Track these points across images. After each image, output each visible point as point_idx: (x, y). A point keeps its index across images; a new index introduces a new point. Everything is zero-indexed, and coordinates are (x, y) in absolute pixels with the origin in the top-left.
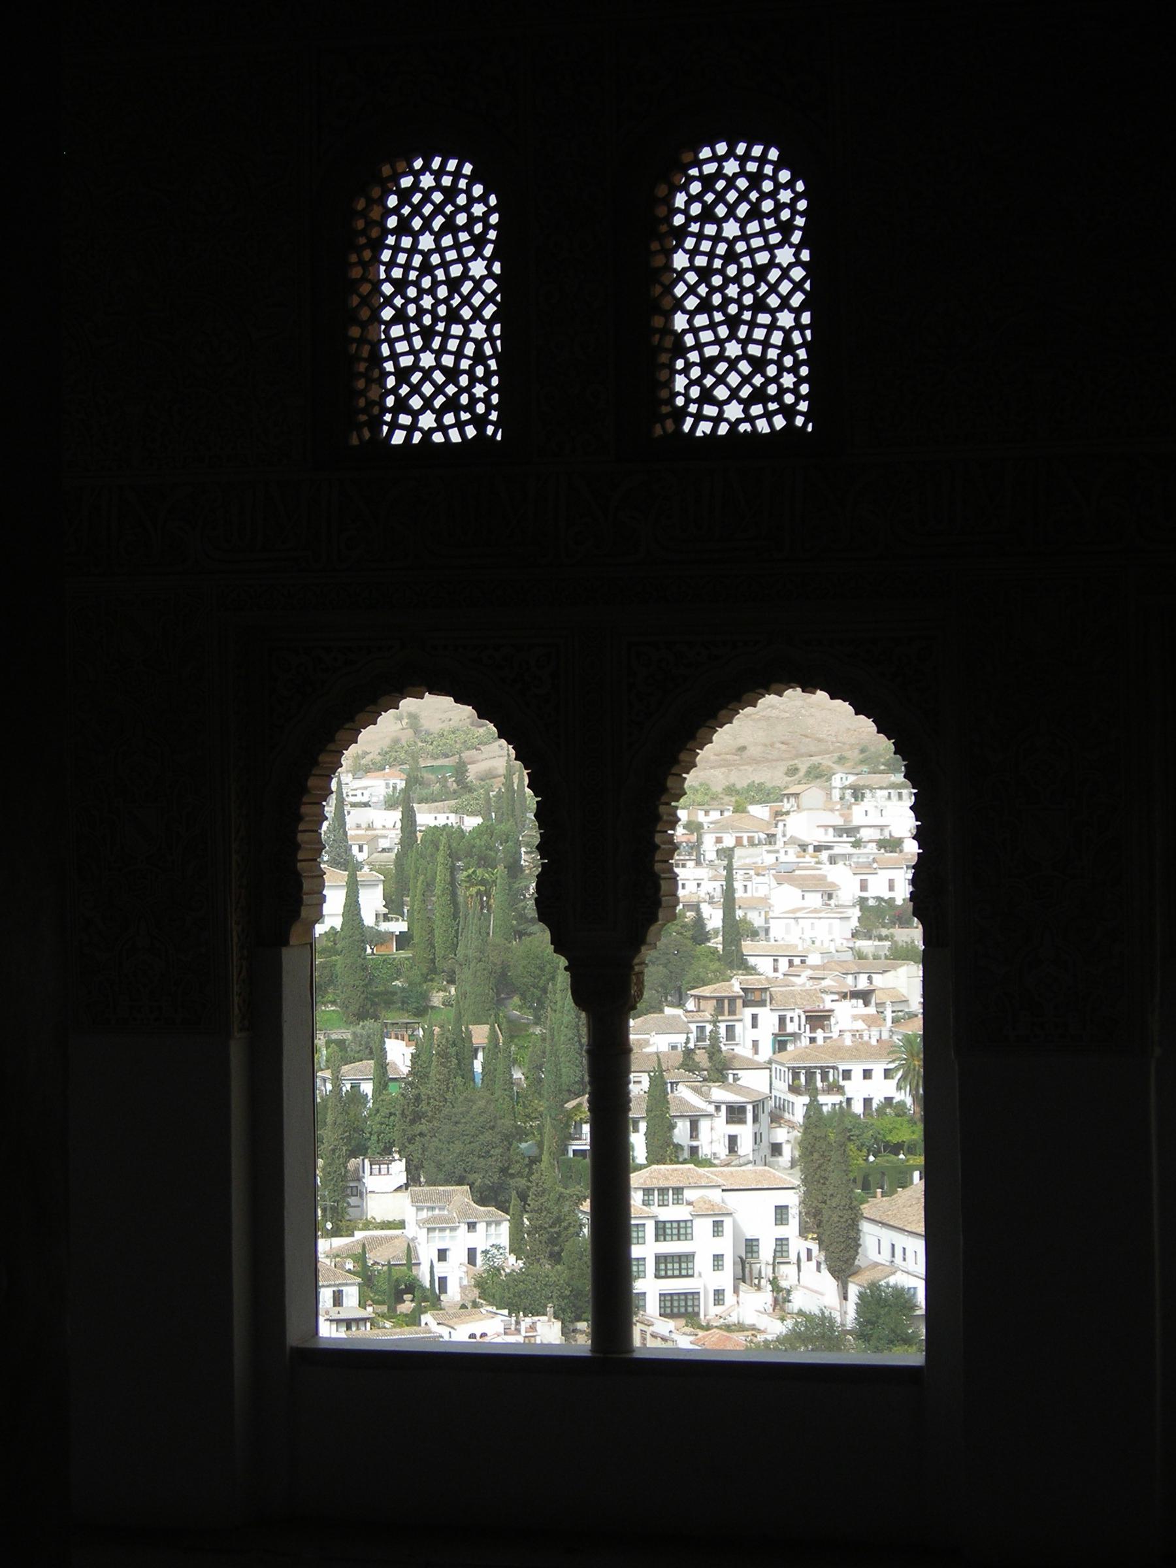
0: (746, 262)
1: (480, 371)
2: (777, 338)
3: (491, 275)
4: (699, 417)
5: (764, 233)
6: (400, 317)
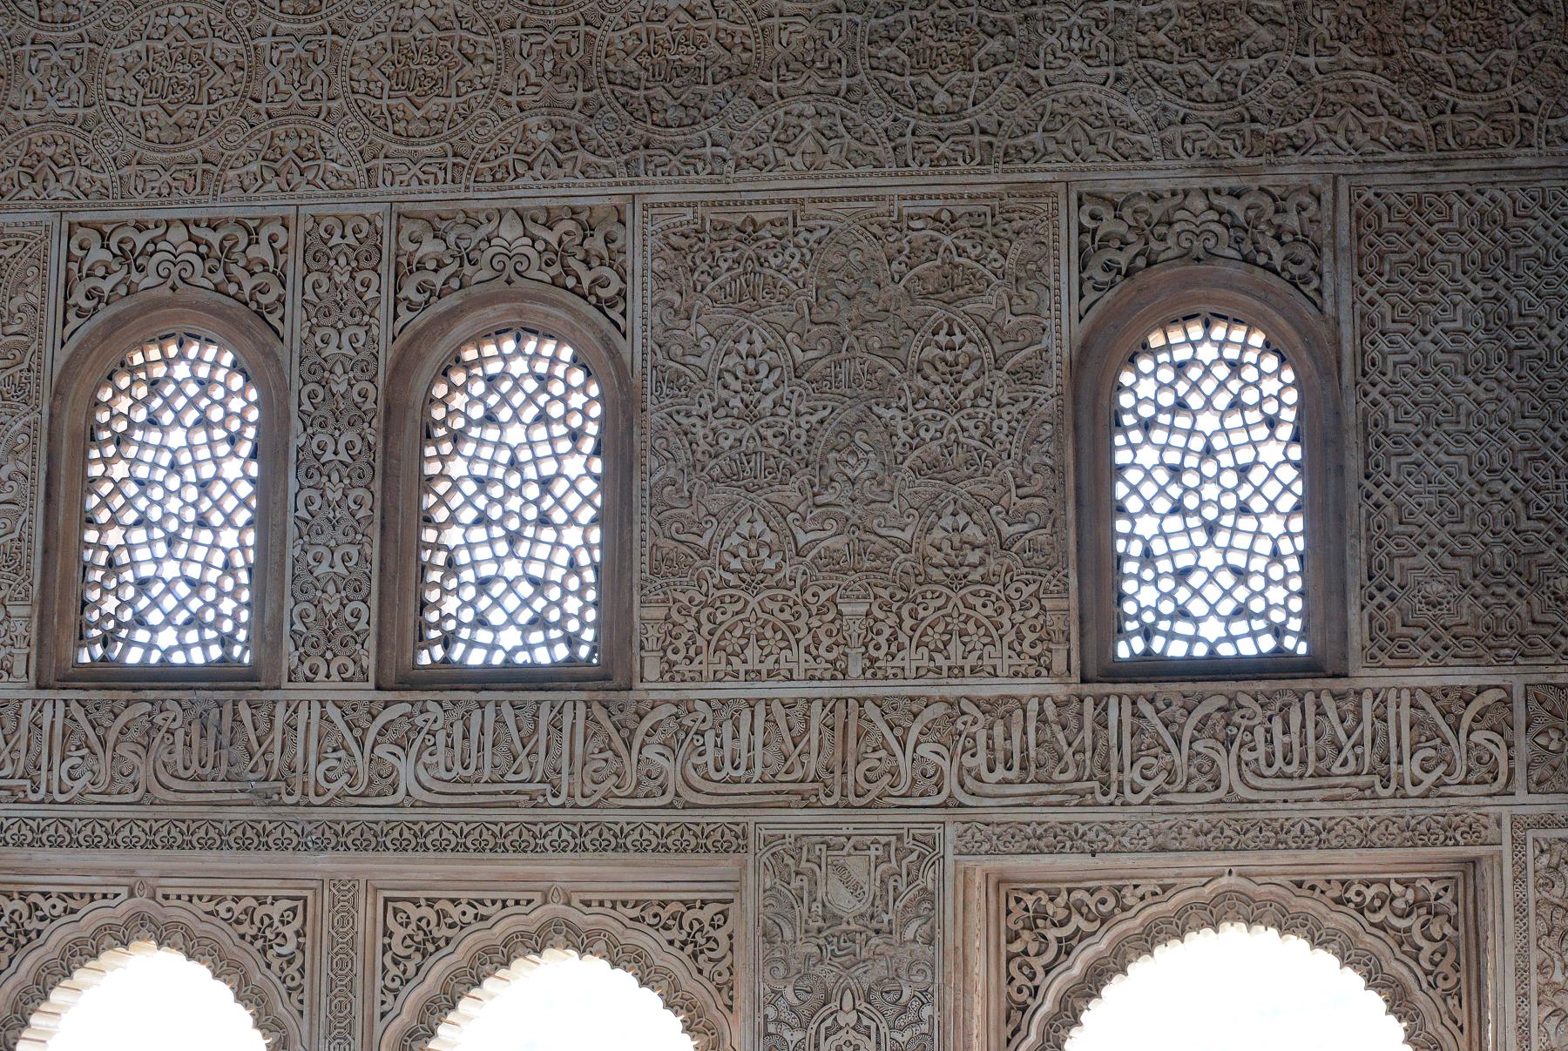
0: (1226, 460)
1: (574, 583)
2: (1264, 546)
3: (589, 473)
4: (1171, 636)
5: (1247, 427)
6: (482, 520)
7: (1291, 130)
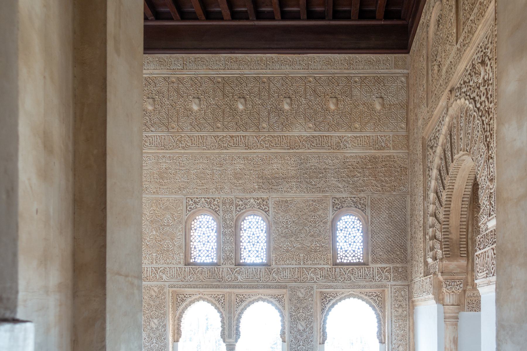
7: (362, 189)
